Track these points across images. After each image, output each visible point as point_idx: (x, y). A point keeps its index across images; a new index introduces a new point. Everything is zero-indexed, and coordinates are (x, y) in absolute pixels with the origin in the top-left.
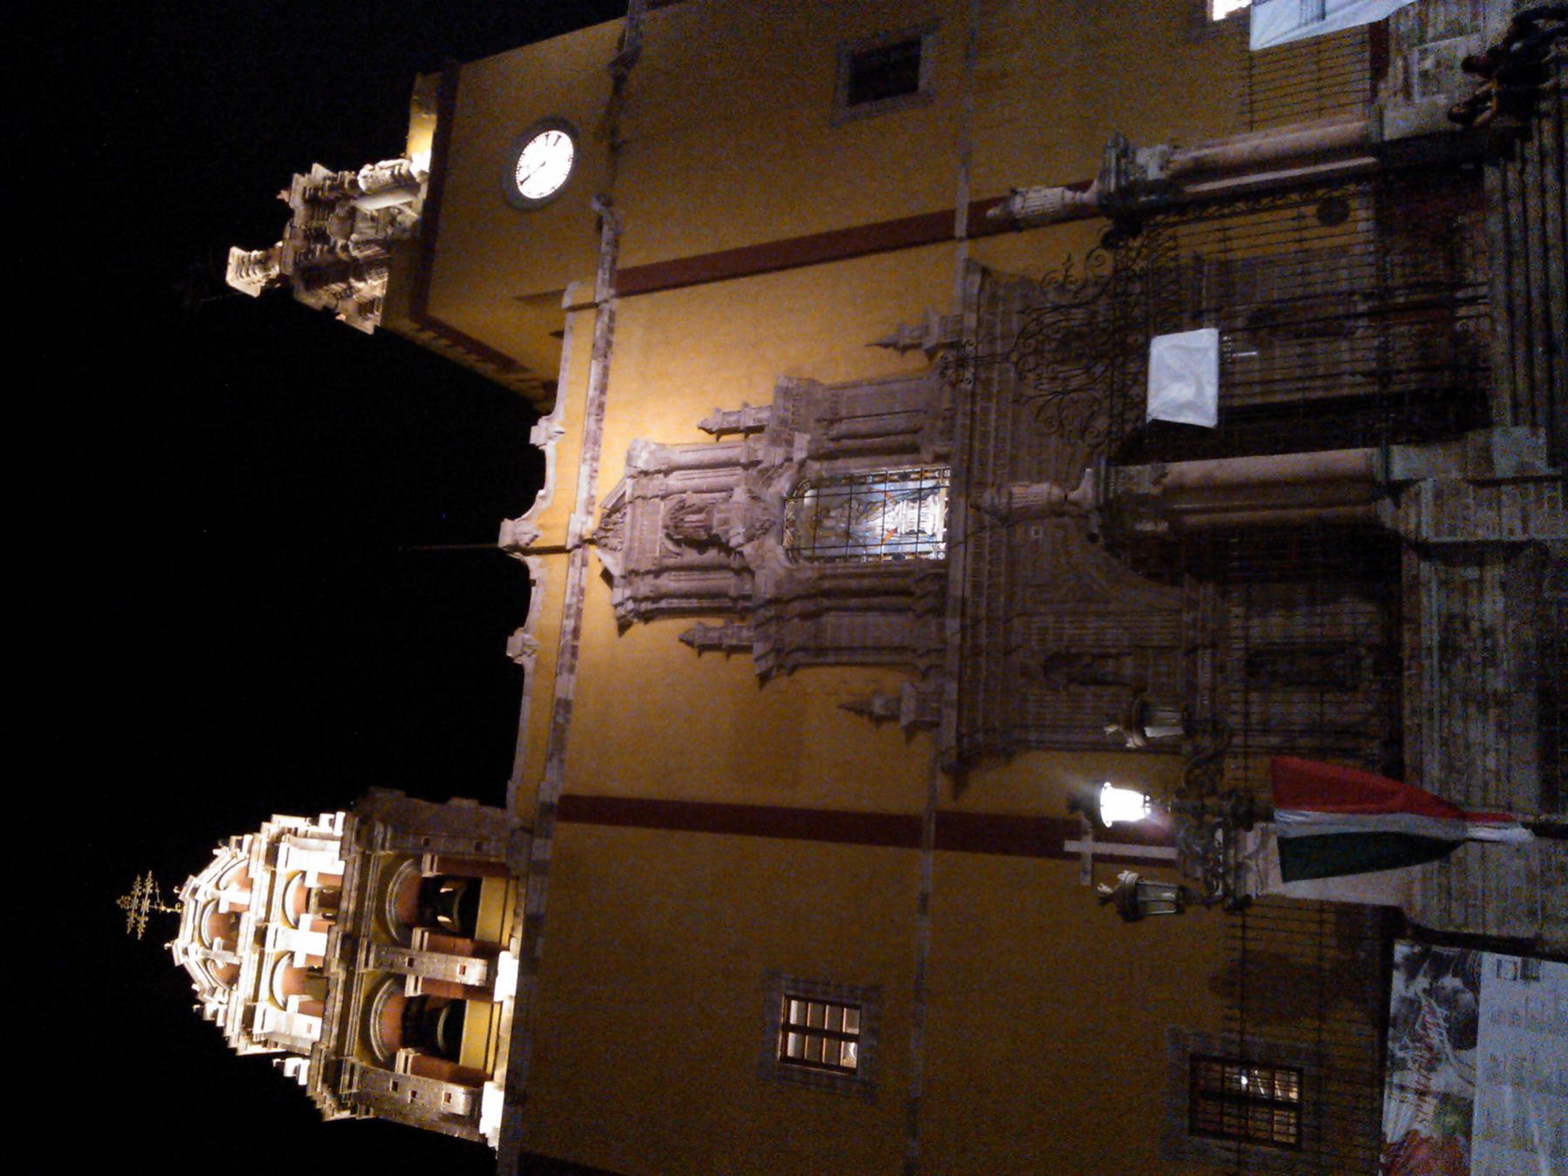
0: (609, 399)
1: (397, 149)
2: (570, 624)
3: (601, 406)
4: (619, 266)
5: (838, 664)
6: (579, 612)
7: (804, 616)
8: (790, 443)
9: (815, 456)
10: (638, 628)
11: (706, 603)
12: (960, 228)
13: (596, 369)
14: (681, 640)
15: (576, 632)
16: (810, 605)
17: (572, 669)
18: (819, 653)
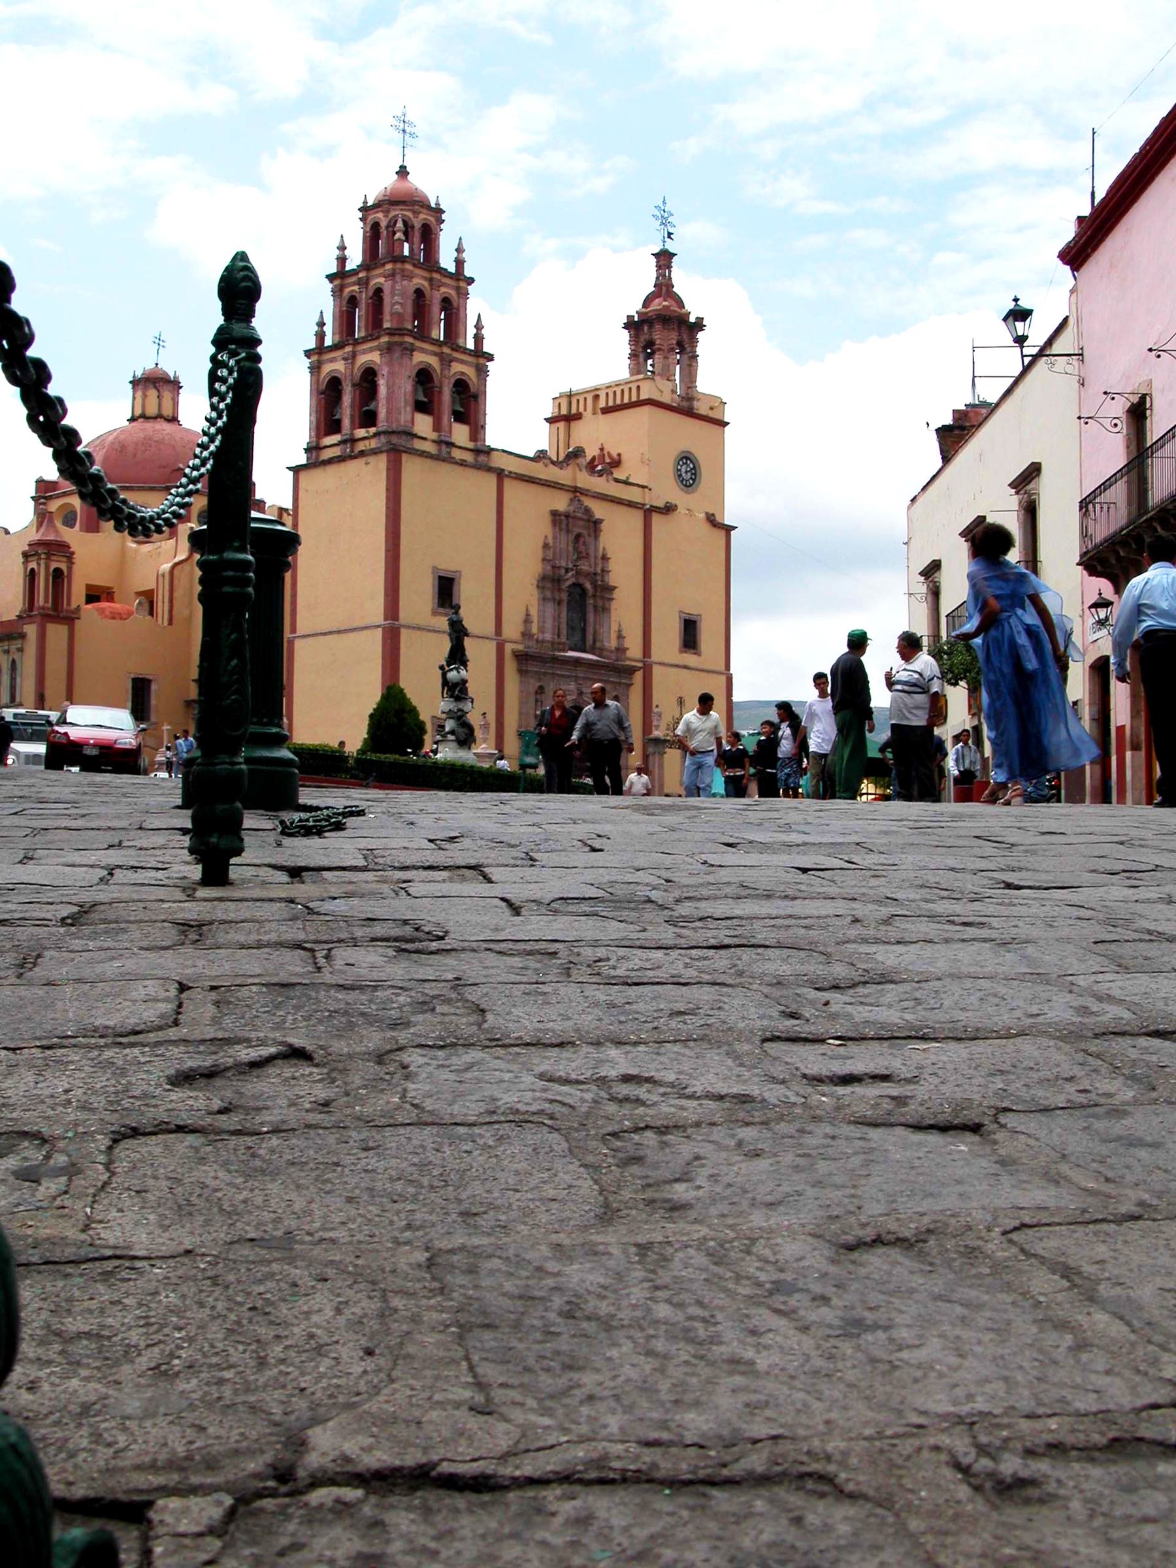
3: (612, 501)
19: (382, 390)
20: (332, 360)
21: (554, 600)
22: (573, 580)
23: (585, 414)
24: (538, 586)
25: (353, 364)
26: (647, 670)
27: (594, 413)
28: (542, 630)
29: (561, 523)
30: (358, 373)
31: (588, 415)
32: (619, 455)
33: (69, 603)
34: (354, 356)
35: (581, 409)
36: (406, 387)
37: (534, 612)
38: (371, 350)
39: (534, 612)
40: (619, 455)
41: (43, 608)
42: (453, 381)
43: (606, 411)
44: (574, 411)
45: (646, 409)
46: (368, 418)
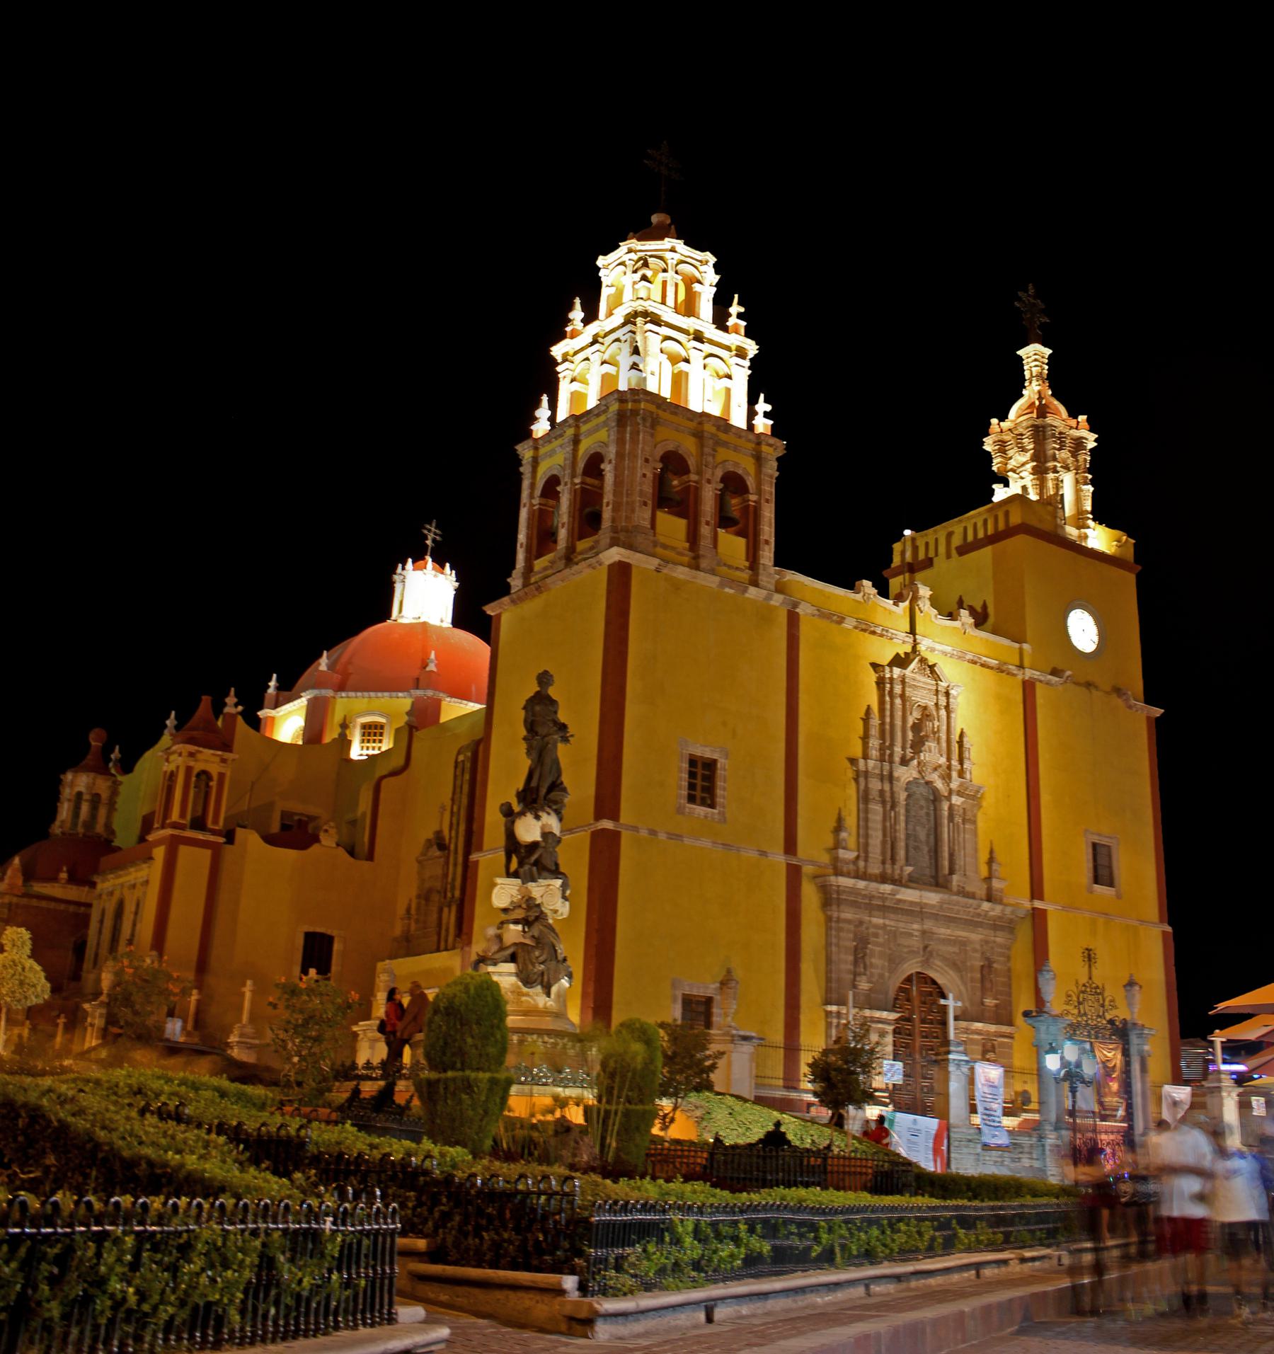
0: (977, 667)
1: (1102, 514)
2: (879, 630)
3: (975, 663)
4: (1038, 685)
5: (858, 810)
6: (882, 636)
7: (882, 792)
8: (959, 794)
9: (951, 807)
10: (873, 677)
11: (887, 727)
12: (1038, 904)
13: (994, 662)
14: (869, 706)
15: (874, 633)
16: (888, 795)
17: (856, 628)
18: (864, 798)
19: (609, 478)
20: (551, 454)
21: (883, 802)
22: (915, 774)
23: (935, 560)
24: (856, 780)
25: (575, 450)
26: (1038, 918)
27: (949, 556)
28: (864, 848)
29: (892, 688)
30: (581, 465)
31: (940, 562)
32: (985, 607)
33: (216, 821)
34: (576, 441)
35: (931, 554)
36: (643, 476)
37: (851, 821)
38: (596, 429)
39: (851, 821)
40: (985, 607)
41: (175, 826)
42: (719, 473)
43: (964, 550)
44: (921, 556)
45: (1021, 540)
46: (588, 520)
